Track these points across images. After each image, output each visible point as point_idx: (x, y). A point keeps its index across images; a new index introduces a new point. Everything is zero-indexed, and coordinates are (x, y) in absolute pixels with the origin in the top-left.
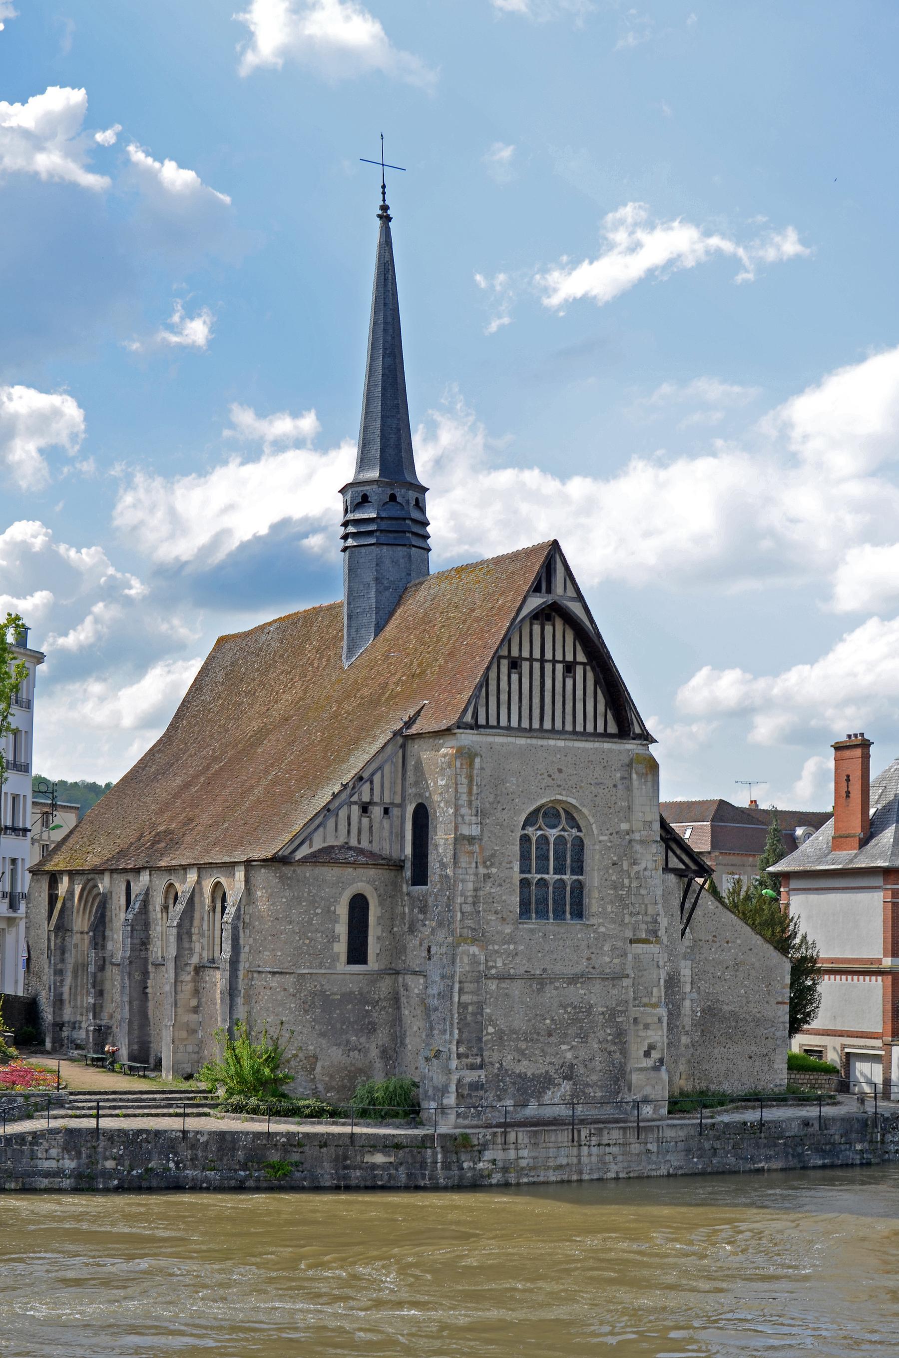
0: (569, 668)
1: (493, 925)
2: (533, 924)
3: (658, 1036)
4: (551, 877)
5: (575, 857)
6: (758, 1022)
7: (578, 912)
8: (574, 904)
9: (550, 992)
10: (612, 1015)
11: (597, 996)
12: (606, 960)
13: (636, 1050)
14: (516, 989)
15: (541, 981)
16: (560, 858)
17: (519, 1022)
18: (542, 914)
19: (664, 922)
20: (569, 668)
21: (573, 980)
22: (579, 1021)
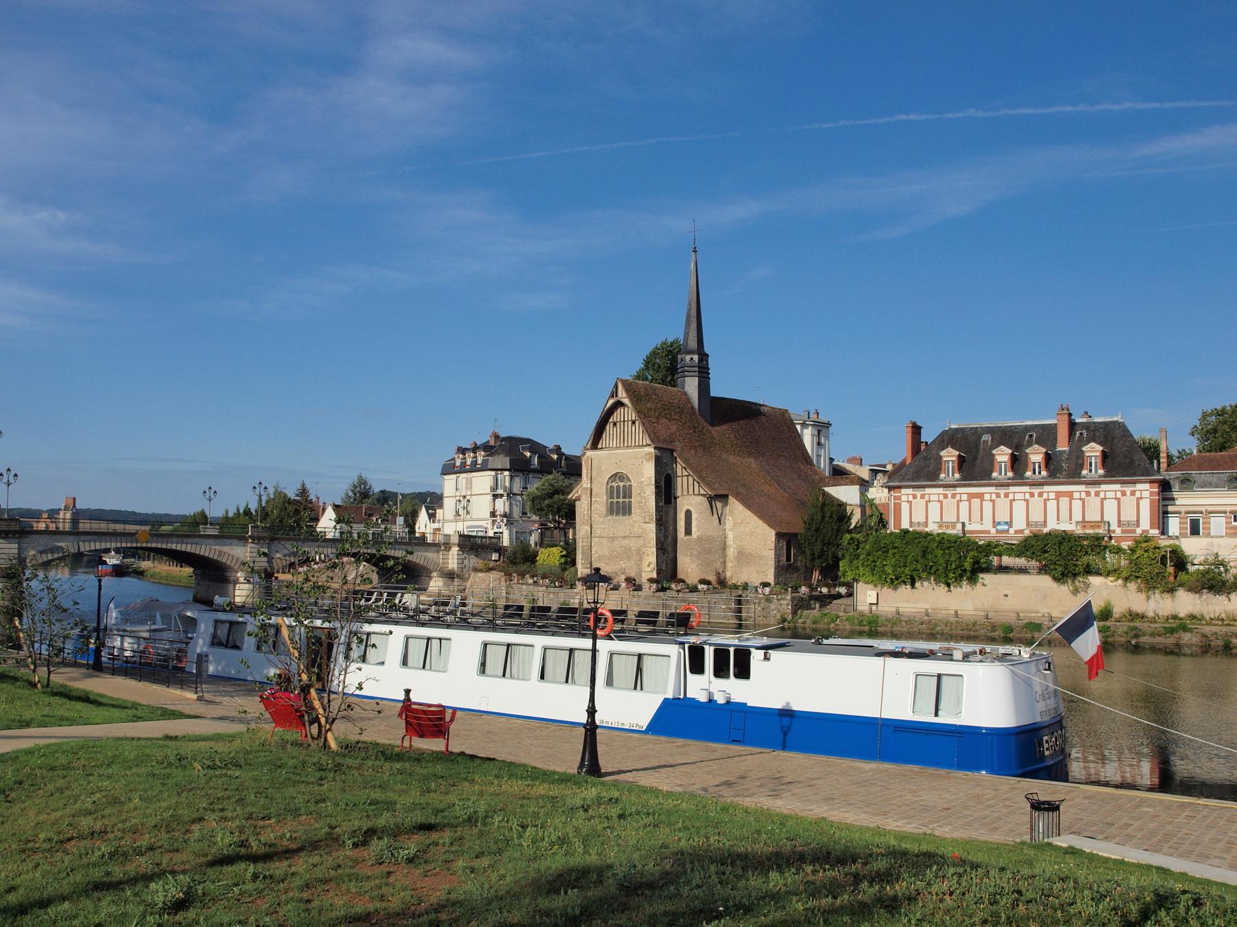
0: (634, 422)
1: (595, 518)
2: (614, 517)
3: (653, 559)
4: (621, 500)
5: (627, 493)
6: (761, 558)
7: (630, 513)
8: (626, 510)
9: (616, 542)
10: (639, 551)
11: (633, 544)
12: (636, 530)
13: (645, 565)
14: (604, 541)
15: (613, 538)
16: (624, 493)
17: (606, 552)
18: (618, 514)
19: (694, 516)
20: (634, 422)
21: (624, 537)
22: (626, 553)
